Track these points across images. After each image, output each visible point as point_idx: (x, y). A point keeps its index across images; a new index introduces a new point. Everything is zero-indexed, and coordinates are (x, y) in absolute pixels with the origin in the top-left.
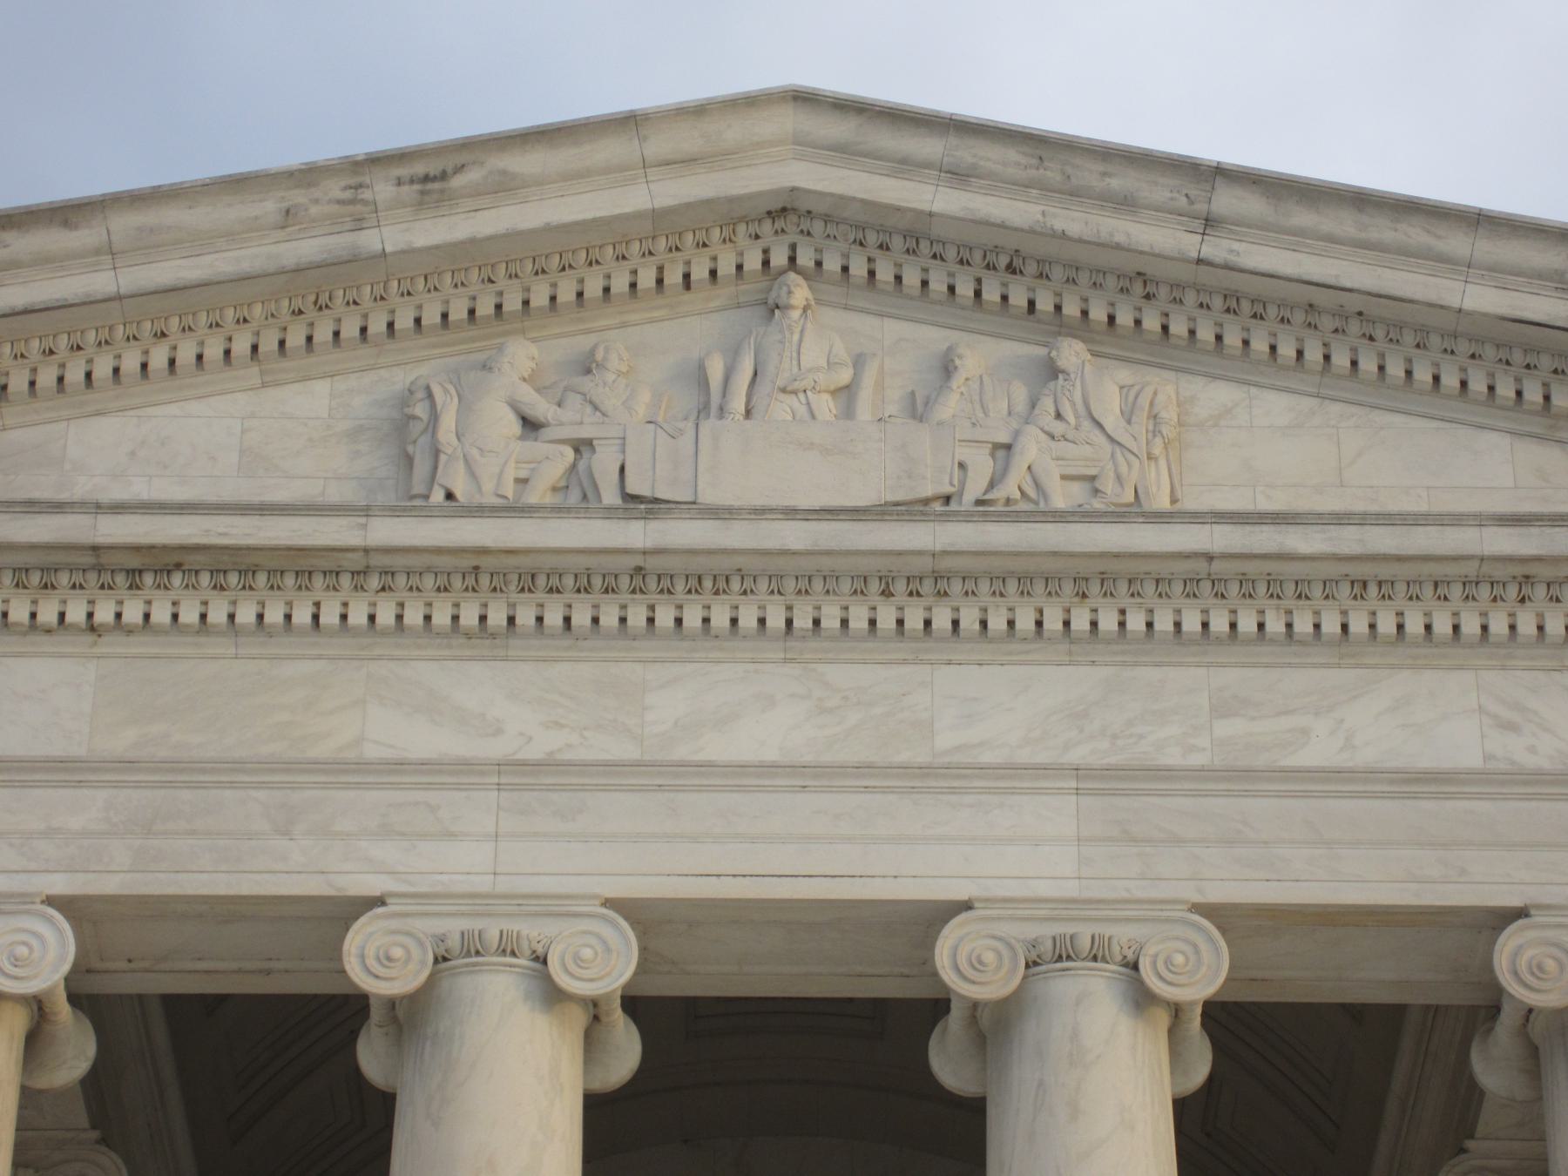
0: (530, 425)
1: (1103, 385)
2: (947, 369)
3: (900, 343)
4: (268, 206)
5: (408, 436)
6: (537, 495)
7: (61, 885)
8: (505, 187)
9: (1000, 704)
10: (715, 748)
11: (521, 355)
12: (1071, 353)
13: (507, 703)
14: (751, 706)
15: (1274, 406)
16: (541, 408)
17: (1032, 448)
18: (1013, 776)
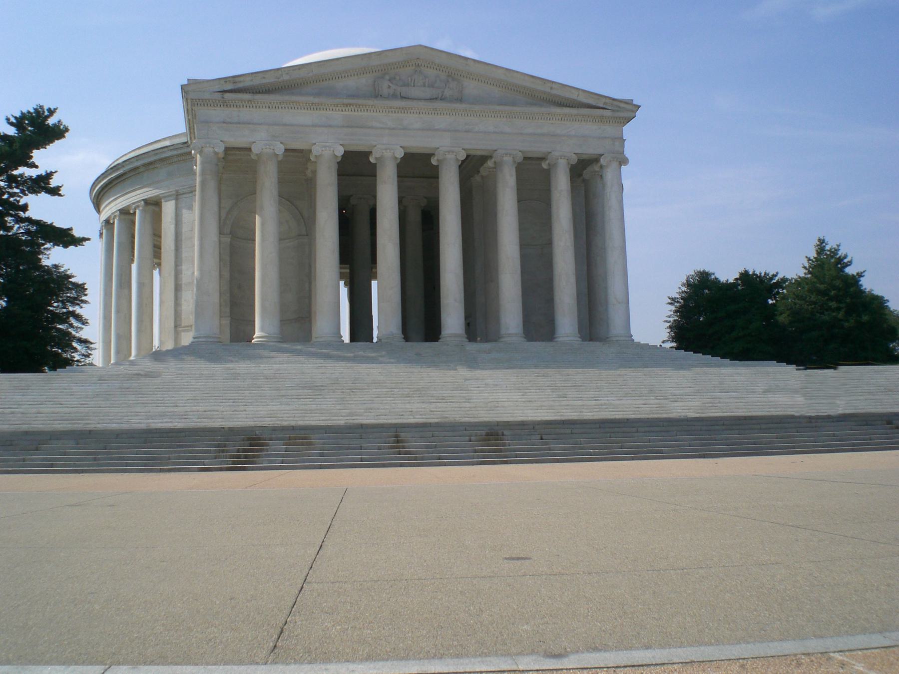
7: (341, 142)
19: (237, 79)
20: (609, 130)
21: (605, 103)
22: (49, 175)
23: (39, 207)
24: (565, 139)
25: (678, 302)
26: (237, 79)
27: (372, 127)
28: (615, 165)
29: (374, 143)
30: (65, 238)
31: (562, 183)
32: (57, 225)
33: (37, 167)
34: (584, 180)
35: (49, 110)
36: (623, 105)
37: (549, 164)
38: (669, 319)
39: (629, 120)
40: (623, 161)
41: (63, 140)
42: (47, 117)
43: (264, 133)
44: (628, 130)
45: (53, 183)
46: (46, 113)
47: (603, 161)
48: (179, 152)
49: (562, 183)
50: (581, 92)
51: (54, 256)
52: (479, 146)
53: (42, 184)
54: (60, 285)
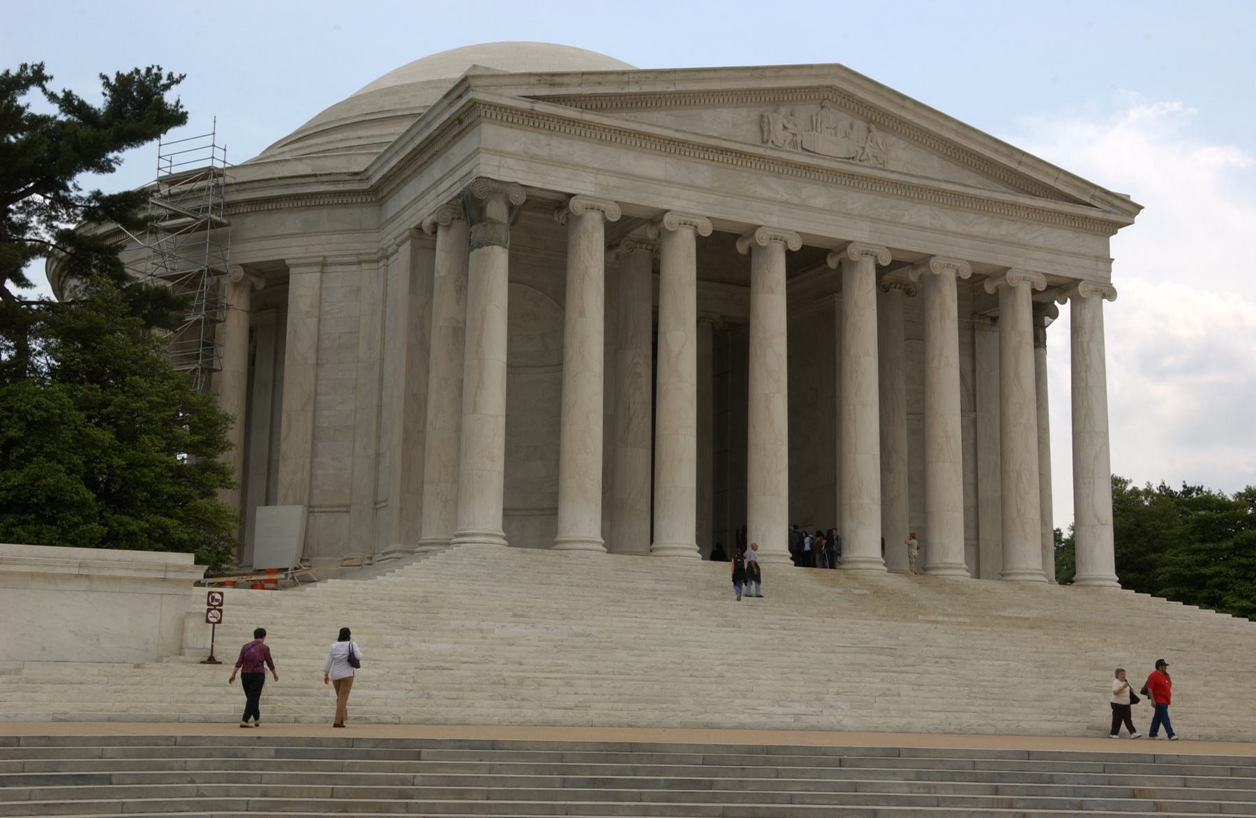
0: (785, 128)
1: (878, 136)
2: (852, 127)
3: (844, 119)
4: (748, 74)
8: (787, 76)
9: (857, 201)
12: (873, 128)
13: (778, 188)
14: (819, 196)
16: (788, 125)
17: (868, 149)
19: (558, 80)
20: (1088, 243)
21: (1093, 197)
26: (558, 80)
29: (759, 223)
36: (1118, 203)
37: (997, 289)
40: (1111, 294)
42: (167, 87)
44: (1121, 244)
46: (164, 81)
47: (1080, 288)
48: (341, 187)
50: (1061, 176)
52: (912, 243)
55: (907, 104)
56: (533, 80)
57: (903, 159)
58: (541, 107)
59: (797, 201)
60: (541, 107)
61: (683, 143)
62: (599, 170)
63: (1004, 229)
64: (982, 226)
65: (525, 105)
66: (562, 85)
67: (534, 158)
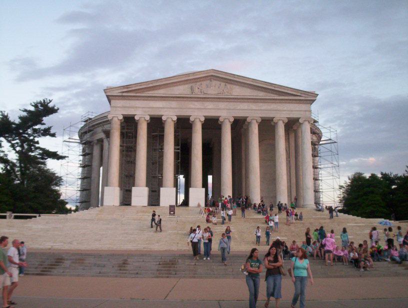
1: (229, 86)
5: (192, 89)
6: (199, 93)
9: (222, 105)
10: (209, 107)
11: (198, 83)
12: (227, 84)
13: (197, 105)
14: (210, 105)
15: (238, 87)
18: (224, 109)
20: (303, 107)
22: (49, 128)
23: (45, 142)
24: (282, 112)
25: (344, 188)
27: (189, 108)
28: (307, 123)
30: (55, 156)
31: (281, 131)
32: (50, 150)
33: (45, 124)
34: (294, 130)
35: (50, 100)
36: (310, 94)
38: (339, 196)
39: (314, 101)
41: (57, 113)
42: (48, 103)
43: (142, 111)
44: (314, 107)
45: (52, 131)
47: (300, 121)
49: (281, 131)
51: (51, 165)
53: (47, 132)
54: (54, 179)
55: (236, 76)
56: (122, 88)
57: (237, 91)
58: (124, 94)
59: (202, 107)
60: (124, 94)
61: (167, 97)
62: (143, 108)
63: (273, 106)
64: (264, 106)
65: (121, 94)
66: (130, 88)
67: (125, 107)
